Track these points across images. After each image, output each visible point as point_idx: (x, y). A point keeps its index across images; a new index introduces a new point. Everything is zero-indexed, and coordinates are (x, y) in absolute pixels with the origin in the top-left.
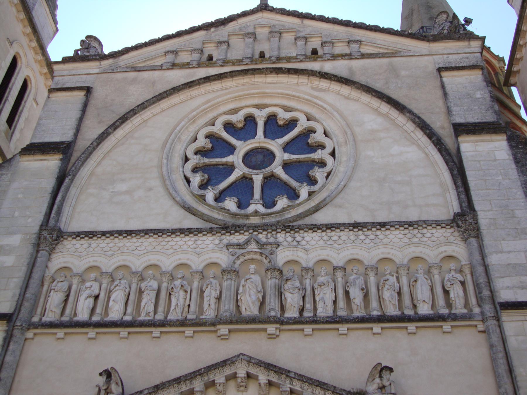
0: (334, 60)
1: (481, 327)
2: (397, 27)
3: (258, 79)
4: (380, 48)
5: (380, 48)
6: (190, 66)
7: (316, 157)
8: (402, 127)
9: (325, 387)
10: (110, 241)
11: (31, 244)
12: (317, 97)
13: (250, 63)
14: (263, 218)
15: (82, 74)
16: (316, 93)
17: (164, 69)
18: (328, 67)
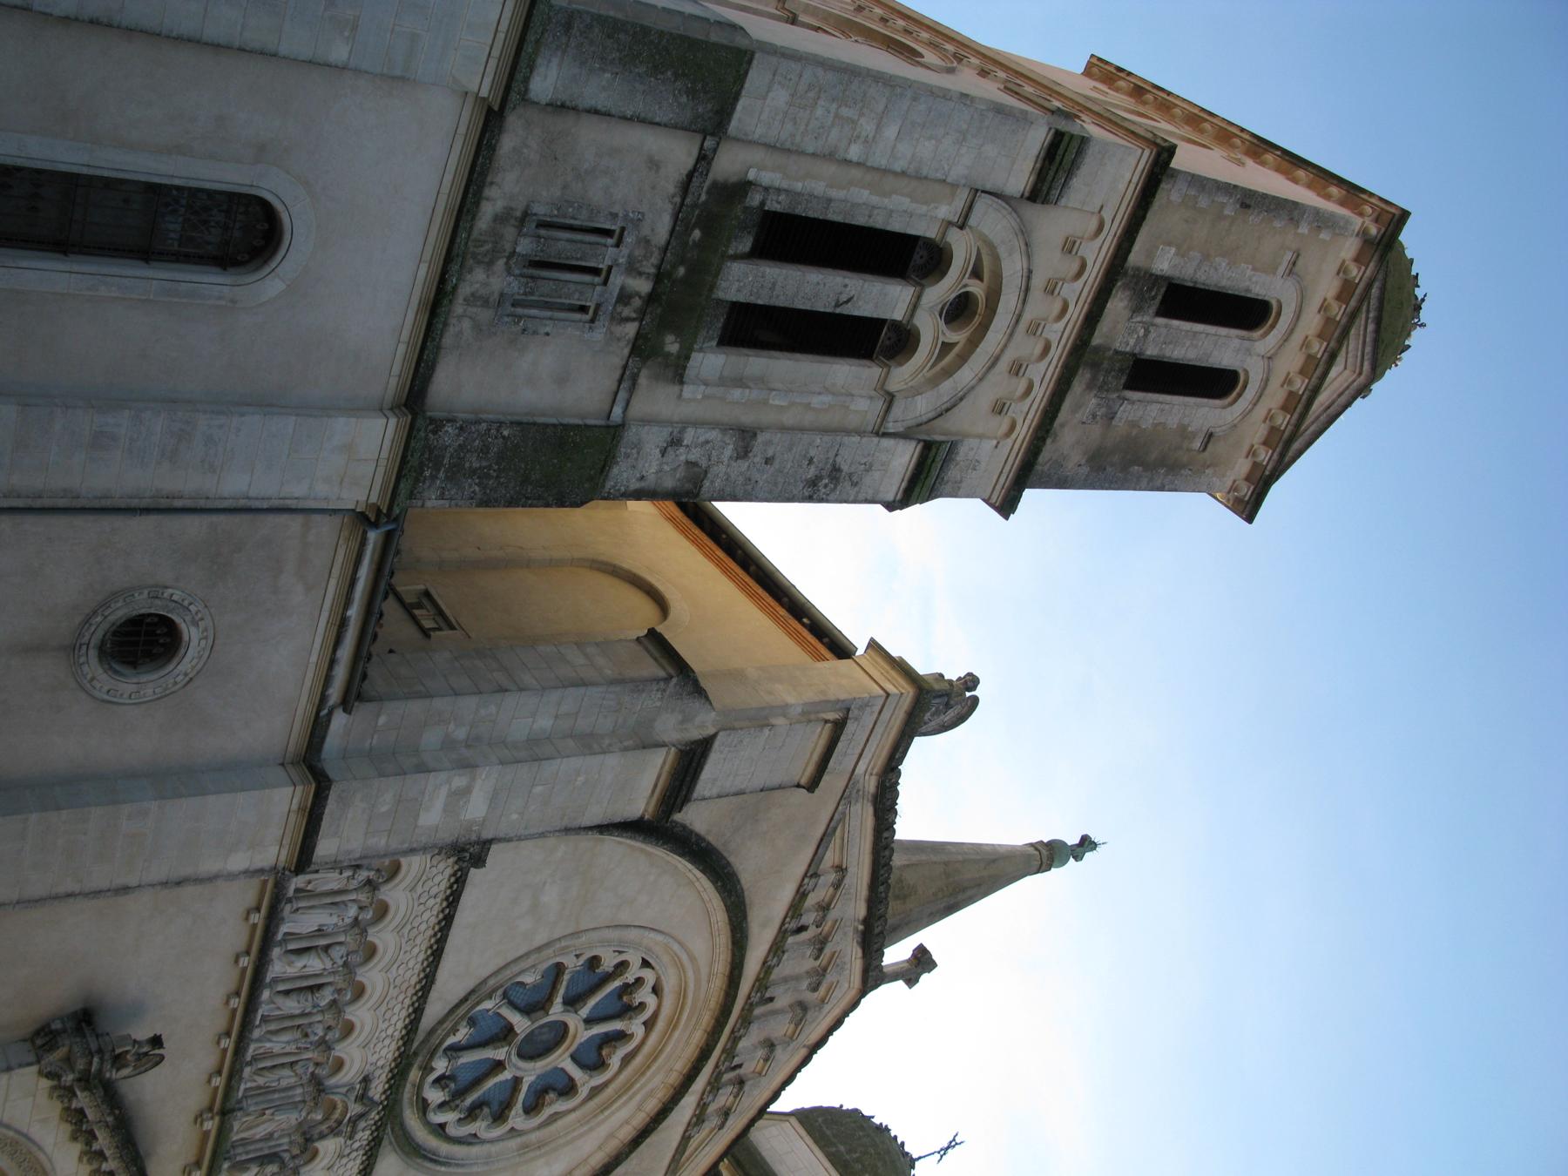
0: (698, 1105)
2: (907, 828)
3: (706, 1020)
4: (696, 1150)
5: (696, 1150)
6: (788, 920)
7: (513, 1113)
11: (458, 836)
12: (631, 1098)
13: (749, 1001)
14: (414, 1085)
16: (643, 1092)
17: (803, 879)
18: (689, 1103)
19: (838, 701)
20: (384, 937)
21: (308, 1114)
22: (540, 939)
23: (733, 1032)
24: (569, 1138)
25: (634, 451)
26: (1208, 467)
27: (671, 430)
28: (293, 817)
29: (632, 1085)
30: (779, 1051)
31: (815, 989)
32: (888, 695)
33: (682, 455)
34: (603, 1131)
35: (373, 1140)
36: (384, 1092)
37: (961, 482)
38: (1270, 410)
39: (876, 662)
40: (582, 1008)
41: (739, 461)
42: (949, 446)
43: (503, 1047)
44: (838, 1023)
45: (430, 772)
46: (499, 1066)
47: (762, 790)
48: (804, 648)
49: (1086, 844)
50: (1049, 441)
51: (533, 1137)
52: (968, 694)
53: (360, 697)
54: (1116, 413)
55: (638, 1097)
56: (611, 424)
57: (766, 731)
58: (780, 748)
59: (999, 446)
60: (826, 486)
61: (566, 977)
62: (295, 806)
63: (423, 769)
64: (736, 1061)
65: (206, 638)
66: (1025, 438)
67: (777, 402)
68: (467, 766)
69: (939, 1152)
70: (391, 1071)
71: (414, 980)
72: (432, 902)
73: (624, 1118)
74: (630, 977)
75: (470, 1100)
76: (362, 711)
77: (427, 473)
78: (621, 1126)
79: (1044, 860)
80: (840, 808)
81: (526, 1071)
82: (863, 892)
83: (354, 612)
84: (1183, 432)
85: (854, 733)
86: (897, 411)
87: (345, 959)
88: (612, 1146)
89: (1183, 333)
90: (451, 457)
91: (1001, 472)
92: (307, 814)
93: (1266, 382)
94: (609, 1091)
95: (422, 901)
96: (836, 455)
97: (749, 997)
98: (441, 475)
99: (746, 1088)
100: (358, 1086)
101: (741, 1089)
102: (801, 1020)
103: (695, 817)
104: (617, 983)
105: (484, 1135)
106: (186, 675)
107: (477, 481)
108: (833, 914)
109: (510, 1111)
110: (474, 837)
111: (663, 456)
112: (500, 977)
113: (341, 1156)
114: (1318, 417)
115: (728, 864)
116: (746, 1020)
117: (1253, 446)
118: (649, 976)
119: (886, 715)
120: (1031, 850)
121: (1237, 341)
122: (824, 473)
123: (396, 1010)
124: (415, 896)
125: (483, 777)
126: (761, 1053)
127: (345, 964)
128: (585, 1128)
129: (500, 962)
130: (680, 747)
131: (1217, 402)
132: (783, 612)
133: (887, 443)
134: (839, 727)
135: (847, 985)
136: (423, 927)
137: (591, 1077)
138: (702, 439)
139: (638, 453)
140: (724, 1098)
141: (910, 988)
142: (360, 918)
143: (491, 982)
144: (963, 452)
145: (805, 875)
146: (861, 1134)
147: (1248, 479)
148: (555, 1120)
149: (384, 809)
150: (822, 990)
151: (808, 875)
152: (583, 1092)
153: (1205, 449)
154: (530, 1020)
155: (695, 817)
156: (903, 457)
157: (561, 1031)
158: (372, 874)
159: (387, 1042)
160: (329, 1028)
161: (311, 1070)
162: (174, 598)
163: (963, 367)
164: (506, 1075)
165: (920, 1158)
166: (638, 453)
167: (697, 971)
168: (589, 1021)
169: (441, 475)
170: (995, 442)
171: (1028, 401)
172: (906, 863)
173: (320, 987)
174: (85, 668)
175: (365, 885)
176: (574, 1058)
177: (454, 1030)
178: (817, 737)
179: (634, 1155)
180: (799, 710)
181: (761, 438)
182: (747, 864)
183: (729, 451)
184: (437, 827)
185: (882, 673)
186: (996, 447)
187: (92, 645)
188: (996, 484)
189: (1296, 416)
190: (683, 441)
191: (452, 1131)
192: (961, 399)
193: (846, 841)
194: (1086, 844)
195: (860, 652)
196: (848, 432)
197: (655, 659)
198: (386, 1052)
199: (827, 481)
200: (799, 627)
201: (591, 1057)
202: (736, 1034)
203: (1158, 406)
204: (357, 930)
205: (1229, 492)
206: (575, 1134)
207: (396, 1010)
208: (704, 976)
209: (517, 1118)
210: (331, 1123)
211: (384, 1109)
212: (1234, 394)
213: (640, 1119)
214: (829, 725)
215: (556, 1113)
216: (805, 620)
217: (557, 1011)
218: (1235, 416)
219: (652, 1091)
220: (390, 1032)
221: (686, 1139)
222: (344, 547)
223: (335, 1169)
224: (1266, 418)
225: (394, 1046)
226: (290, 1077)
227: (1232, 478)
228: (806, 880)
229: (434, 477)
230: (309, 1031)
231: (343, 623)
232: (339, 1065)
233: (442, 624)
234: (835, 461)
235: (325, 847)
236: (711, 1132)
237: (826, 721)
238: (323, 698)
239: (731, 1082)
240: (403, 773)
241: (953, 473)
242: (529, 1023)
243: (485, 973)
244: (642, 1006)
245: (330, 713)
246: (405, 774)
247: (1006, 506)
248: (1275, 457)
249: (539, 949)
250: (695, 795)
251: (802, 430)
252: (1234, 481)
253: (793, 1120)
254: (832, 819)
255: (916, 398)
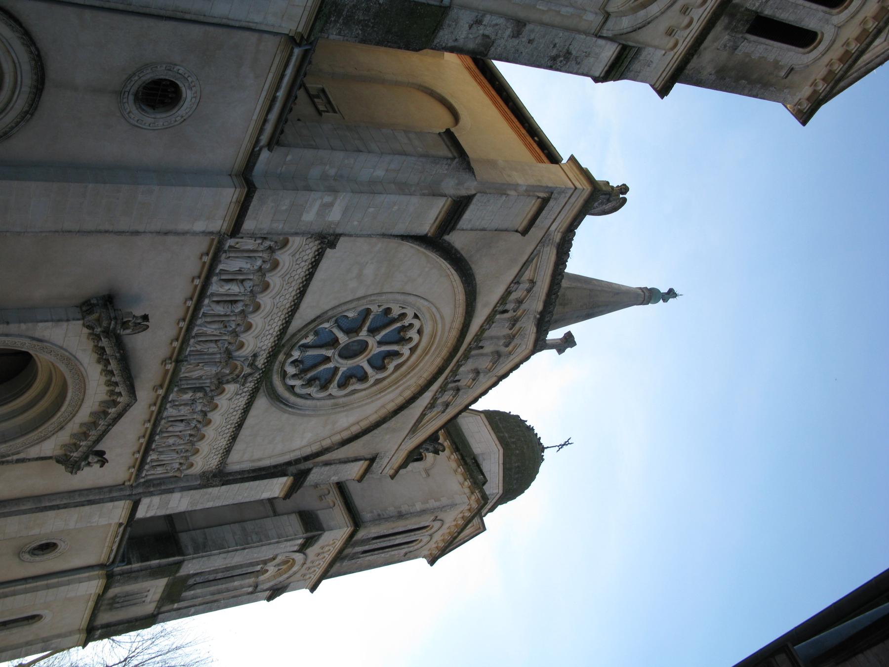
0: (432, 398)
1: (127, 483)
2: (573, 266)
3: (445, 352)
4: (428, 422)
5: (428, 422)
6: (498, 305)
7: (332, 386)
8: (330, 437)
9: (96, 443)
10: (301, 276)
11: (323, 229)
12: (397, 388)
13: (470, 346)
14: (280, 363)
15: (558, 215)
19: (547, 187)
20: (274, 279)
21: (222, 369)
22: (360, 293)
23: (458, 362)
24: (360, 404)
25: (454, 24)
26: (787, 88)
27: (477, 14)
28: (232, 206)
29: (398, 382)
30: (482, 375)
31: (507, 346)
32: (576, 188)
33: (481, 30)
34: (379, 403)
35: (255, 388)
36: (264, 364)
37: (639, 72)
38: (832, 60)
39: (573, 169)
40: (377, 335)
41: (514, 39)
42: (636, 49)
43: (331, 349)
44: (516, 367)
45: (312, 191)
46: (327, 359)
47: (496, 230)
48: (533, 154)
49: (671, 294)
50: (695, 57)
51: (341, 401)
52: (621, 196)
53: (278, 143)
54: (739, 46)
55: (401, 388)
56: (443, 5)
57: (504, 197)
58: (510, 208)
59: (666, 54)
60: (561, 62)
61: (371, 317)
62: (234, 200)
63: (308, 188)
64: (457, 378)
65: (195, 97)
66: (681, 53)
67: (541, 7)
68: (333, 191)
69: (558, 446)
70: (269, 353)
71: (288, 305)
72: (303, 264)
73: (391, 398)
74: (406, 322)
75: (309, 375)
76: (279, 151)
77: (333, 19)
78: (389, 402)
79: (646, 298)
80: (538, 247)
81: (342, 364)
82: (543, 296)
83: (281, 94)
84: (776, 65)
85: (553, 206)
86: (610, 24)
87: (252, 288)
88: (383, 412)
89: (790, 4)
90: (348, 11)
91: (664, 70)
92: (240, 205)
93: (833, 42)
94: (385, 383)
95: (298, 262)
96: (570, 44)
97: (470, 344)
98: (341, 21)
99: (460, 393)
100: (250, 358)
101: (457, 394)
102: (497, 361)
103: (457, 239)
104: (399, 325)
105: (314, 395)
106: (182, 117)
107: (361, 28)
108: (524, 306)
109: (330, 385)
110: (331, 231)
111: (470, 28)
112: (335, 311)
113: (237, 394)
114: (860, 69)
115: (470, 268)
116: (466, 356)
117: (816, 80)
118: (417, 324)
119: (573, 200)
120: (640, 291)
121: (821, 14)
122: (561, 54)
123: (276, 321)
124: (294, 259)
125: (341, 198)
126: (471, 376)
127: (251, 291)
128: (370, 400)
129: (336, 303)
130: (454, 198)
131: (801, 50)
132: (524, 131)
133: (601, 42)
134: (545, 202)
135: (524, 347)
136: (297, 277)
137: (377, 373)
138: (494, 22)
139: (456, 25)
140: (447, 397)
141: (559, 354)
142: (263, 267)
143: (330, 313)
144: (644, 54)
145: (512, 282)
146: (518, 429)
147: (808, 99)
148: (354, 393)
149: (284, 208)
150: (510, 348)
151: (514, 282)
152: (371, 381)
153: (786, 78)
154: (348, 337)
155: (457, 239)
156: (608, 52)
157: (364, 346)
158: (272, 244)
159: (269, 337)
160: (238, 325)
161: (226, 346)
162: (180, 72)
163: (653, 4)
164: (331, 365)
165: (548, 447)
166: (456, 25)
167: (444, 325)
168: (380, 343)
169: (341, 21)
170: (664, 52)
171: (688, 31)
172: (569, 286)
173: (236, 302)
174: (126, 105)
175: (267, 249)
176: (369, 361)
177: (306, 336)
178: (531, 206)
179: (393, 419)
180: (524, 188)
181: (529, 27)
182: (481, 269)
183: (508, 32)
184: (312, 222)
185: (575, 176)
186: (664, 55)
187: (131, 93)
188: (660, 77)
189: (846, 66)
190: (482, 22)
191: (298, 390)
192: (649, 23)
193: (538, 267)
194: (671, 294)
195: (564, 161)
196: (579, 32)
197: (448, 146)
198: (267, 343)
199: (562, 59)
200: (532, 142)
201: (379, 363)
202: (460, 363)
203: (765, 46)
204: (260, 274)
205: (795, 106)
206: (364, 402)
207: (276, 321)
208: (447, 328)
209: (333, 389)
210: (234, 376)
211: (263, 372)
212: (812, 47)
213: (400, 400)
214: (540, 200)
215: (355, 390)
216: (536, 138)
217: (363, 334)
218: (809, 60)
219: (409, 386)
220: (271, 332)
221: (423, 415)
222: (280, 55)
223: (233, 400)
224: (828, 65)
225: (272, 340)
226: (214, 348)
227: (799, 98)
228: (512, 285)
229: (336, 22)
230: (228, 324)
231: (274, 99)
232: (241, 345)
233: (330, 109)
234: (568, 48)
235: (249, 225)
236: (437, 414)
237: (539, 197)
238: (258, 141)
239: (452, 389)
240: (296, 189)
241: (636, 66)
242: (347, 339)
243: (327, 308)
244: (410, 339)
245: (260, 150)
246: (298, 190)
247: (663, 91)
248: (828, 89)
249: (359, 299)
250: (458, 227)
251: (553, 26)
252: (800, 100)
253: (482, 415)
254: (532, 253)
255: (623, 18)
